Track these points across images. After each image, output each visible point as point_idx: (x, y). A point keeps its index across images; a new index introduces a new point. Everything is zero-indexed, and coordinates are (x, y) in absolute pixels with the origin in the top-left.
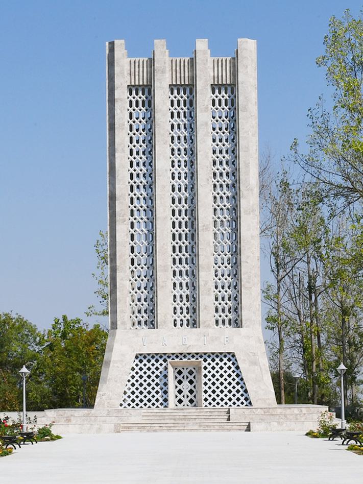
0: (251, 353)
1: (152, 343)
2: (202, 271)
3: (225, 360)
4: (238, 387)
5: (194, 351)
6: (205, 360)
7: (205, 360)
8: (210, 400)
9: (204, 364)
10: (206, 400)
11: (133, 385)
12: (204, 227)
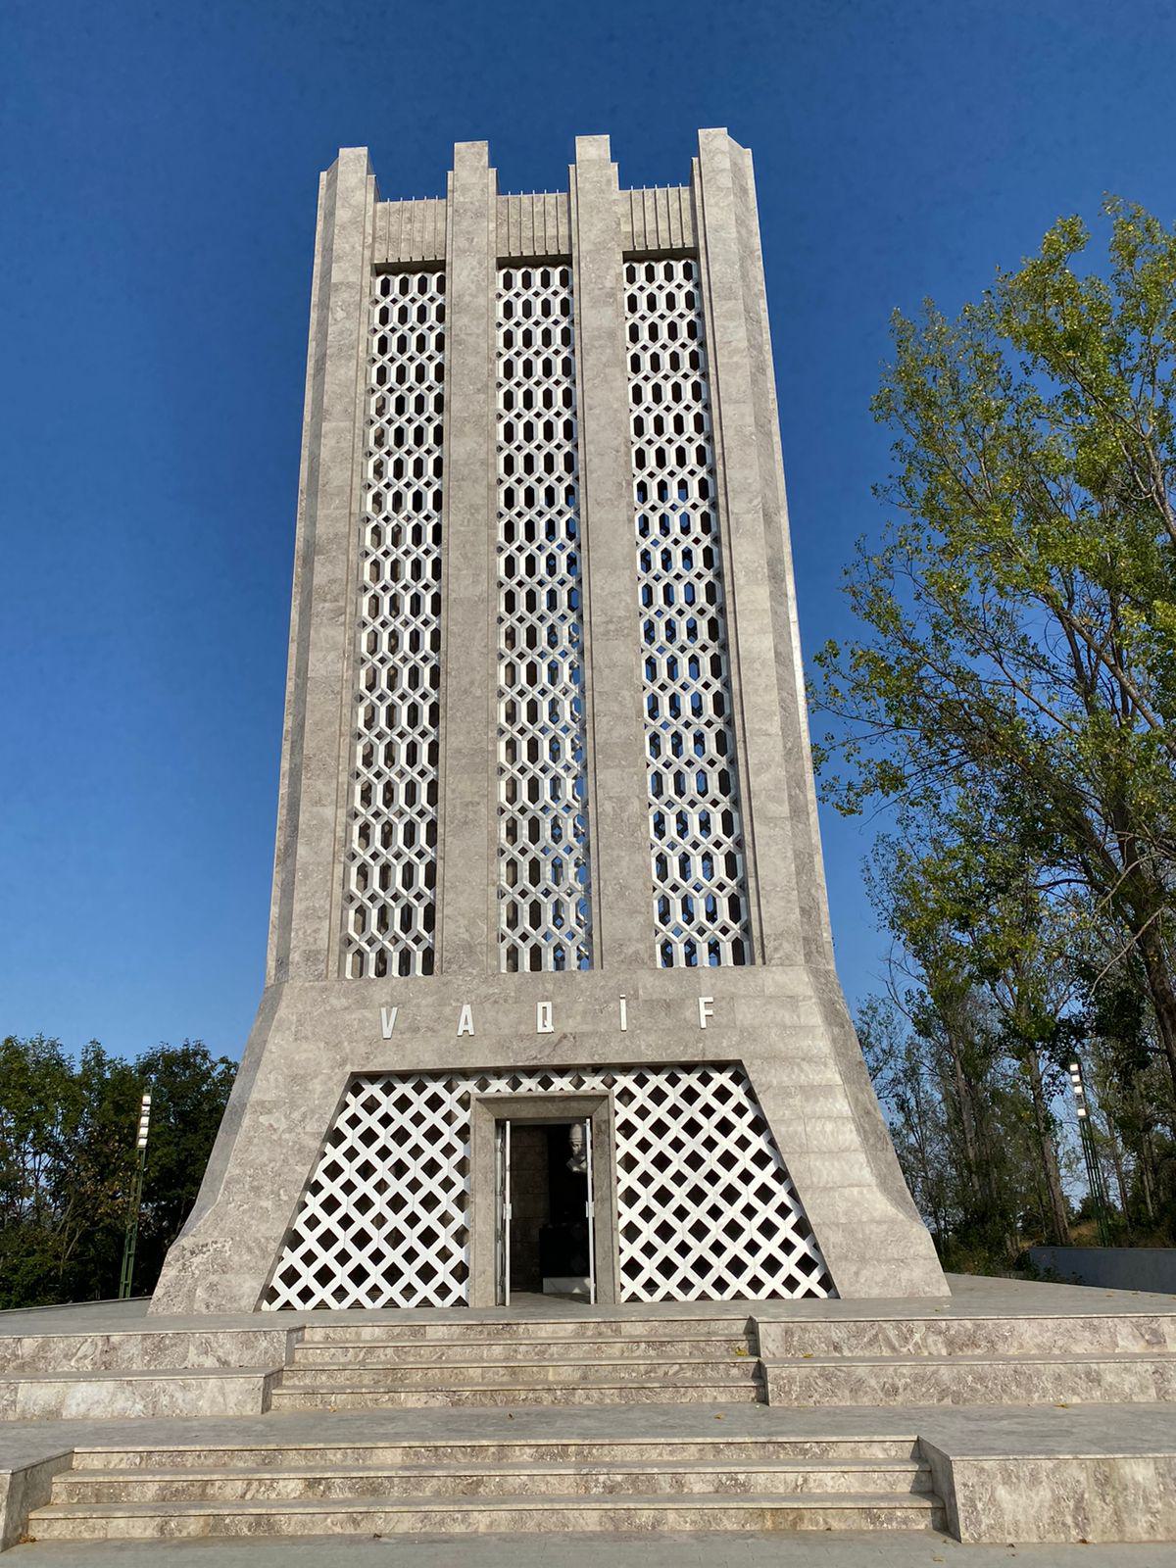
1: (417, 1030)
2: (608, 767)
12: (611, 627)
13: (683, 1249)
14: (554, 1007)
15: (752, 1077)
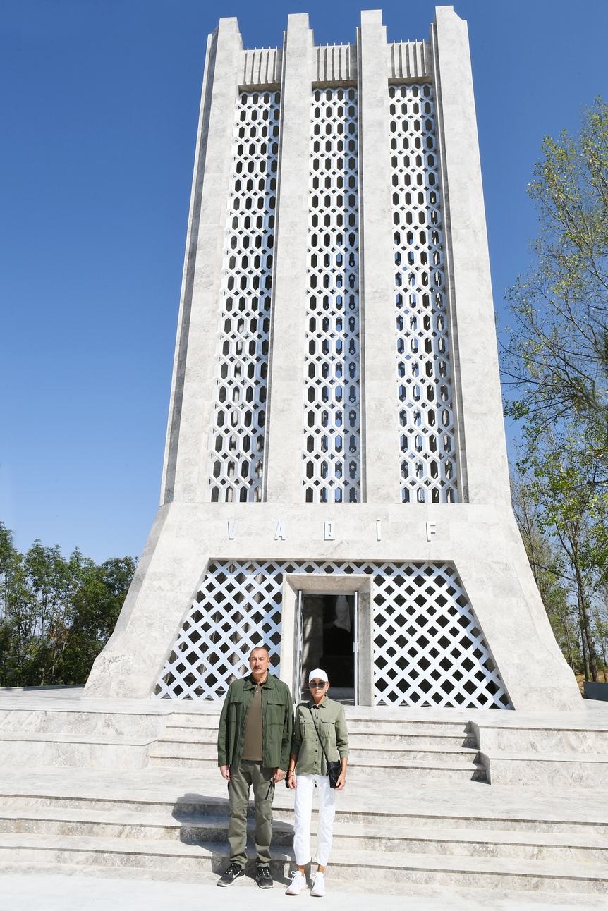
0: (497, 563)
3: (430, 581)
4: (467, 653)
5: (351, 555)
6: (379, 581)
7: (379, 581)
8: (392, 685)
9: (376, 590)
10: (381, 685)
11: (195, 637)
12: (377, 295)
13: (414, 675)
14: (336, 524)
15: (460, 571)
